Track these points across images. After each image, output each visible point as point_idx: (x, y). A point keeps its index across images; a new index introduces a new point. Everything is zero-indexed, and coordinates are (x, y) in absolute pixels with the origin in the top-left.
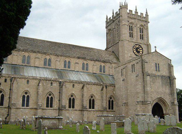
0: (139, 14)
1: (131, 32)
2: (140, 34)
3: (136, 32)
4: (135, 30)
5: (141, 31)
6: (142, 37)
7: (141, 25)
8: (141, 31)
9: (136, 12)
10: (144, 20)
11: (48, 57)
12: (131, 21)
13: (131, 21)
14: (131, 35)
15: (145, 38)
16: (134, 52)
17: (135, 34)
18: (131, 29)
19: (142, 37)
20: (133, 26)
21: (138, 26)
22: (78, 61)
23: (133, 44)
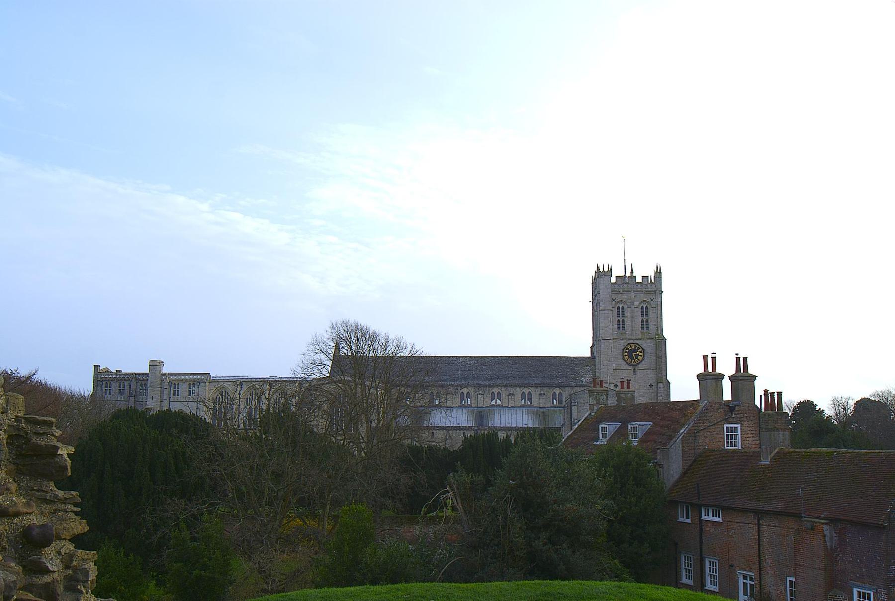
0: (639, 280)
1: (621, 319)
2: (641, 319)
3: (634, 319)
4: (628, 313)
5: (645, 312)
6: (645, 325)
7: (644, 301)
8: (645, 312)
9: (633, 277)
10: (652, 288)
11: (465, 391)
12: (619, 297)
13: (619, 297)
14: (621, 325)
15: (652, 327)
16: (623, 359)
17: (628, 323)
18: (621, 313)
19: (645, 325)
20: (626, 306)
21: (637, 304)
22: (512, 391)
23: (623, 343)
